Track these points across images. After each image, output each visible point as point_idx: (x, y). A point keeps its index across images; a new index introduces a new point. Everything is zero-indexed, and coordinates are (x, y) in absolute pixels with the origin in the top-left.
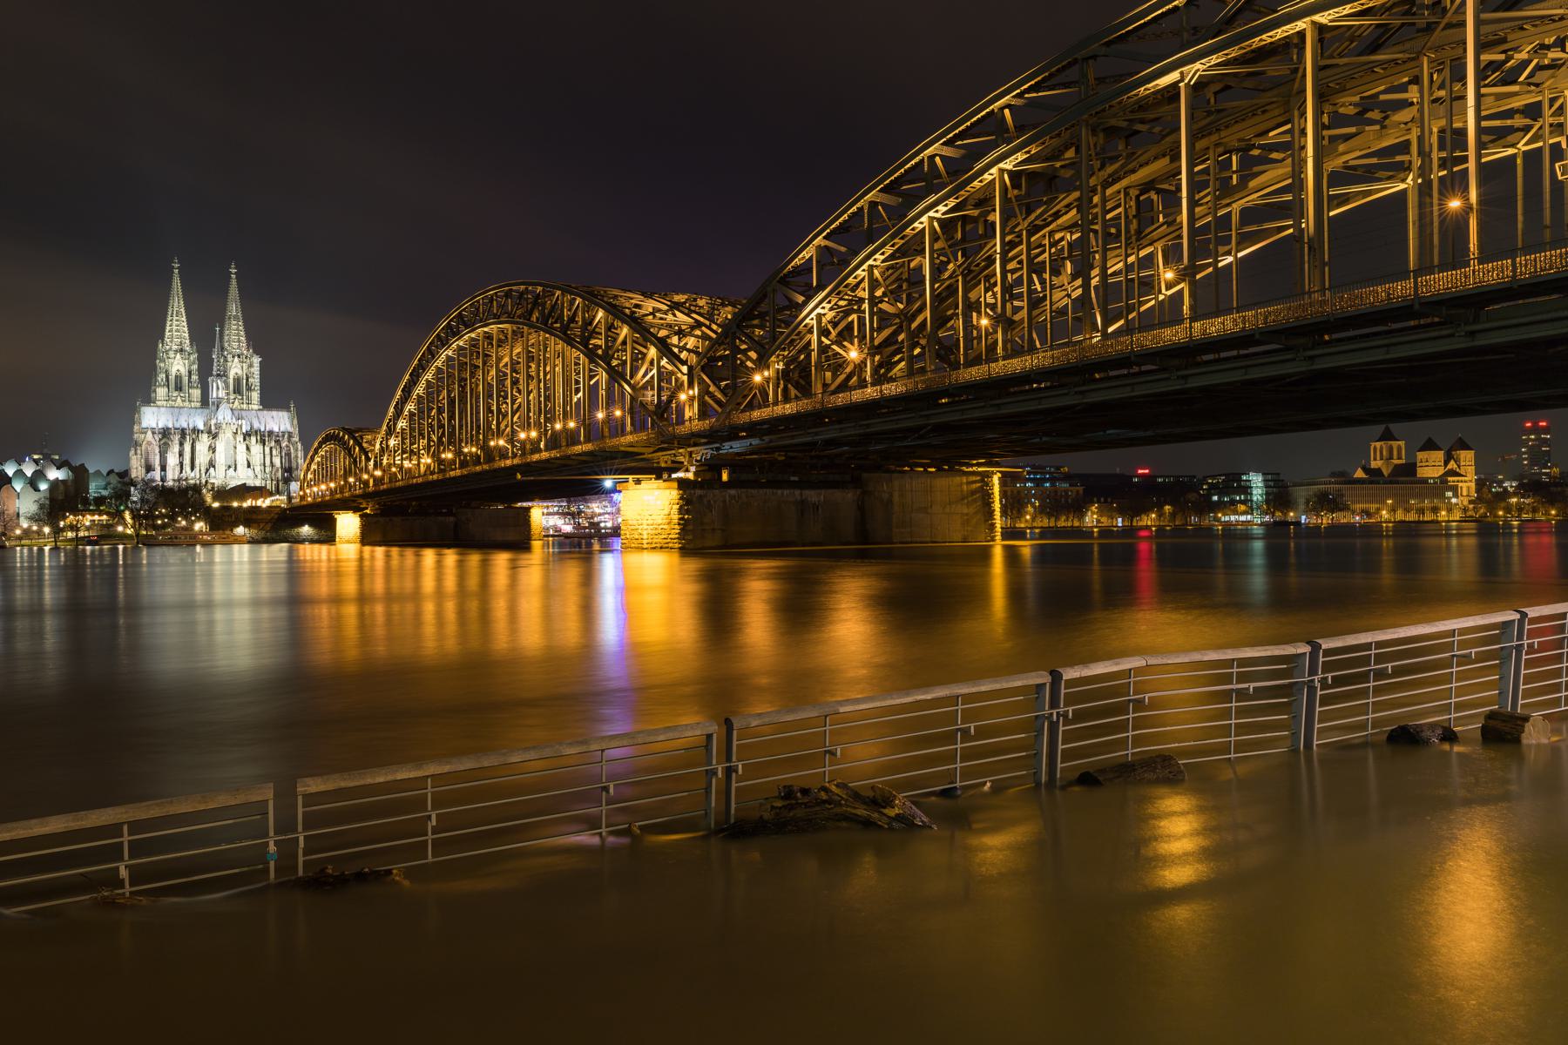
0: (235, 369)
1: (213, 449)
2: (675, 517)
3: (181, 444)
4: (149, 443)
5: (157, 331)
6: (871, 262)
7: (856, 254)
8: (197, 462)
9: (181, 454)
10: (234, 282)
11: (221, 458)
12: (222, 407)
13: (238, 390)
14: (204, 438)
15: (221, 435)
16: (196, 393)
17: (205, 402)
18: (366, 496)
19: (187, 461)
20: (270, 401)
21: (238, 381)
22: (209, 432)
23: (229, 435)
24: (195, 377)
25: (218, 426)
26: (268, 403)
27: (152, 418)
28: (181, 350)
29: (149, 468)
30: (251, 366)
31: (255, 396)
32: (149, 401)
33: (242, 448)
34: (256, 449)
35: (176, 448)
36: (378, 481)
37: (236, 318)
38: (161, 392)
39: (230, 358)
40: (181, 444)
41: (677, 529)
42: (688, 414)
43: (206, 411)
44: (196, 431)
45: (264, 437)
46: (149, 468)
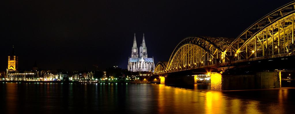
1: (140, 65)
2: (221, 80)
3: (135, 64)
5: (132, 46)
7: (254, 33)
11: (141, 67)
12: (142, 58)
16: (138, 55)
17: (139, 57)
18: (166, 74)
19: (136, 67)
21: (144, 53)
22: (140, 62)
23: (143, 62)
26: (148, 57)
27: (131, 60)
29: (131, 68)
31: (147, 55)
32: (130, 57)
33: (145, 65)
34: (147, 65)
35: (135, 65)
36: (168, 71)
38: (132, 55)
40: (135, 64)
41: (221, 82)
42: (223, 61)
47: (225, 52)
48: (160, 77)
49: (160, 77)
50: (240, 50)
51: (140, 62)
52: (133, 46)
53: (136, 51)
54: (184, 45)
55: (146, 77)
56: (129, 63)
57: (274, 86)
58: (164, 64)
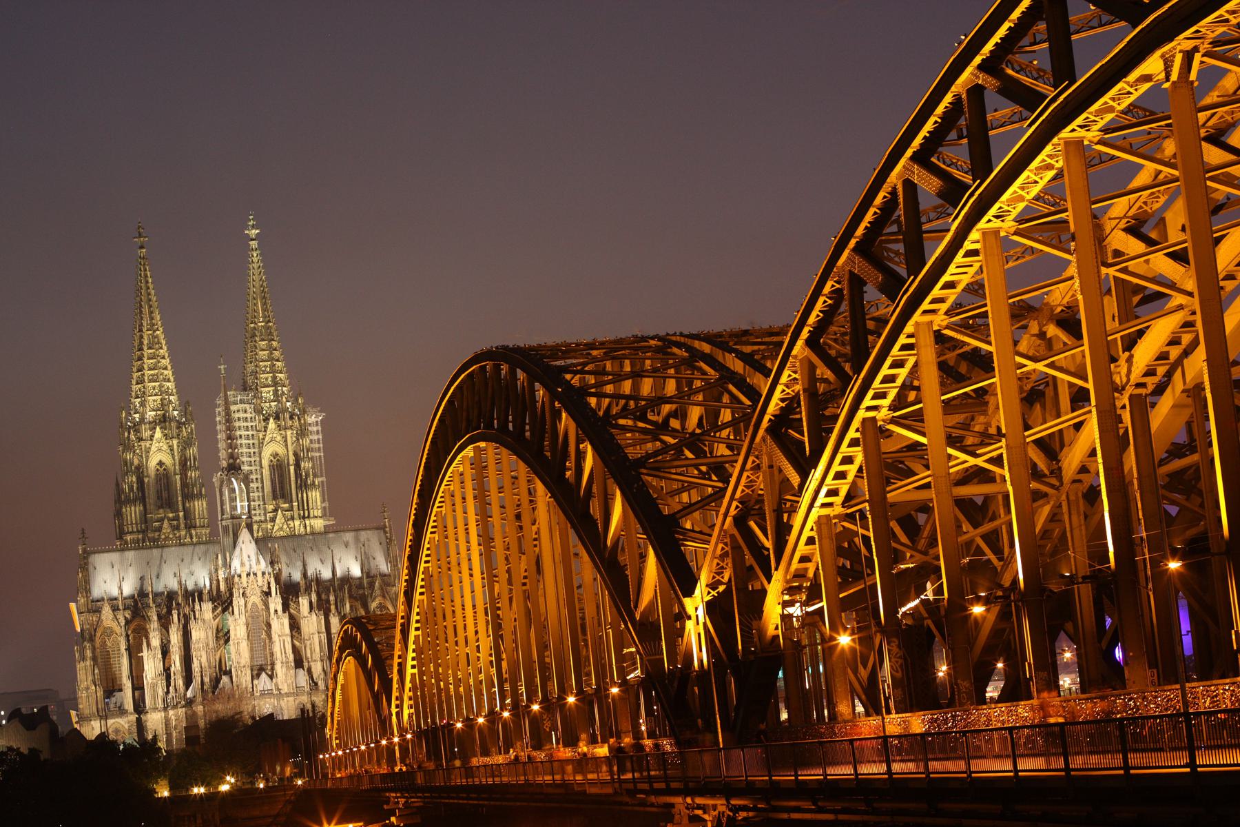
1: (223, 636)
4: (109, 632)
6: (861, 414)
9: (165, 652)
11: (240, 653)
12: (244, 535)
14: (207, 607)
15: (238, 602)
21: (278, 467)
23: (255, 599)
28: (163, 420)
29: (111, 688)
30: (302, 433)
31: (315, 496)
33: (280, 625)
34: (311, 624)
35: (156, 642)
43: (213, 549)
44: (195, 596)
45: (328, 593)
50: (790, 590)
51: (223, 601)
52: (135, 388)
53: (167, 460)
54: (469, 451)
58: (372, 647)
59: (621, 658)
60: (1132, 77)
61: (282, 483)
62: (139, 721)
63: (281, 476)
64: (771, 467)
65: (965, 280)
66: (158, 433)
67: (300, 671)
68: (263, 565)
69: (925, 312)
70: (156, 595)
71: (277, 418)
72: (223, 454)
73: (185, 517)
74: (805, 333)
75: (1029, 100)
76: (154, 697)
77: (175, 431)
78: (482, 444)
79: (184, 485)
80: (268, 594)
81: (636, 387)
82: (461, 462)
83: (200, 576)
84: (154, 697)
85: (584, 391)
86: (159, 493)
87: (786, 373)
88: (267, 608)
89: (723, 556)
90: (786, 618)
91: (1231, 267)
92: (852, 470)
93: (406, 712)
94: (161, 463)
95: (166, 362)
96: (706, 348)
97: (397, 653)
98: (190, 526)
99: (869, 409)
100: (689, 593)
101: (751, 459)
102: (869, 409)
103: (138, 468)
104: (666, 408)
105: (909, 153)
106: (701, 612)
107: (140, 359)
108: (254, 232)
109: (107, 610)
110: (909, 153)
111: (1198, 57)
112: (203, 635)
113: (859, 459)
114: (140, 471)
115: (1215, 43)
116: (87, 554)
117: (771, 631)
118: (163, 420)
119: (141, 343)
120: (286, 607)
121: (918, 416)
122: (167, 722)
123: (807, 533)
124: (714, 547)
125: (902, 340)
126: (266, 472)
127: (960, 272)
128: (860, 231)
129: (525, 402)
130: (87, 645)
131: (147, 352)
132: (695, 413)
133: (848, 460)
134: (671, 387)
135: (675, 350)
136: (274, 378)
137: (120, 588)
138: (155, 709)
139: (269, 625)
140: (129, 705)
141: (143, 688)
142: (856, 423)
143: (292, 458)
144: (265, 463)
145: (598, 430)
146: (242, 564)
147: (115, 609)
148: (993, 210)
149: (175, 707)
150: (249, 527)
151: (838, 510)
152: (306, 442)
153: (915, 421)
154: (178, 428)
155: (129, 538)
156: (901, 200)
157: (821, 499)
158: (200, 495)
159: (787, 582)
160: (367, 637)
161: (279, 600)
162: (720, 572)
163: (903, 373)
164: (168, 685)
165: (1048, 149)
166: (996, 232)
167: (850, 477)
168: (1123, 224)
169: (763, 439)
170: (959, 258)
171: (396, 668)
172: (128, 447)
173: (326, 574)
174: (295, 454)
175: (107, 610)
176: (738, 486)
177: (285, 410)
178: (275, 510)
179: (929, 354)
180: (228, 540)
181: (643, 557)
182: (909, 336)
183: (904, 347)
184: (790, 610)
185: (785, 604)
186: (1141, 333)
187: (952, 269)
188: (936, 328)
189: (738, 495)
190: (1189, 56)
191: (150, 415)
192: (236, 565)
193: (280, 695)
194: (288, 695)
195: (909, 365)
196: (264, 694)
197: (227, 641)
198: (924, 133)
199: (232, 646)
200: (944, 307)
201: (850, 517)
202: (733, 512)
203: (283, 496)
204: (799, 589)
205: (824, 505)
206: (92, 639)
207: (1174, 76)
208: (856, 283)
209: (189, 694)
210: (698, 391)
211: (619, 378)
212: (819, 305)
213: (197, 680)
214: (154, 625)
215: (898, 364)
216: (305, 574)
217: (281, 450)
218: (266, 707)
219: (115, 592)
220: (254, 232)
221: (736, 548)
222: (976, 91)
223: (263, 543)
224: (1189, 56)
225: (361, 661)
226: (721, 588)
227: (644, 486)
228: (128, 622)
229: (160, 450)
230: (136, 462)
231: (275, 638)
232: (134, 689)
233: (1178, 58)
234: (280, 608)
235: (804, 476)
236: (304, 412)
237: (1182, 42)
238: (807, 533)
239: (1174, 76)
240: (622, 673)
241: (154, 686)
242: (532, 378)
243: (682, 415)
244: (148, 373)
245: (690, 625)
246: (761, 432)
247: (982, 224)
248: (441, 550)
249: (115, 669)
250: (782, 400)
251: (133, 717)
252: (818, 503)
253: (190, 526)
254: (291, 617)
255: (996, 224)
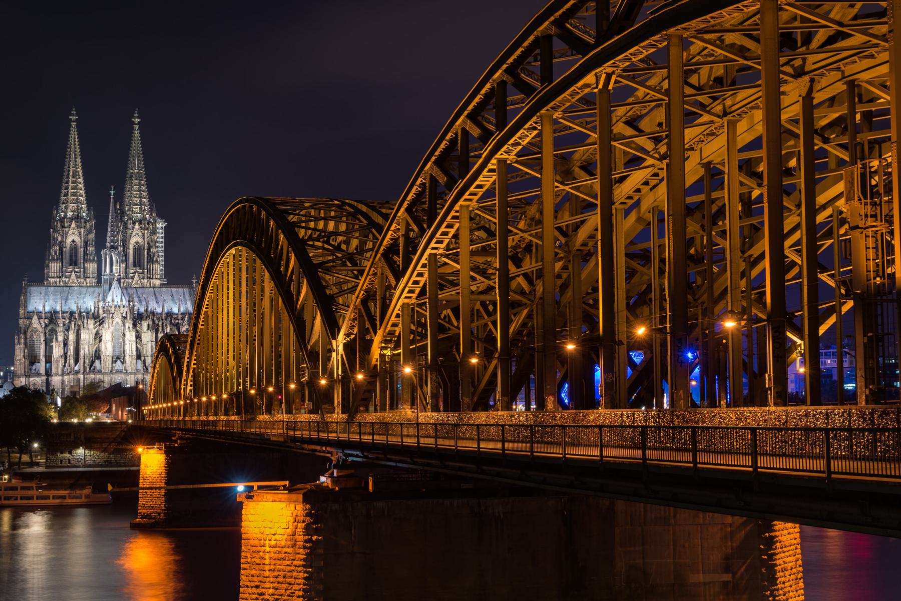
0: (136, 238)
1: (98, 337)
2: (300, 538)
6: (429, 251)
8: (82, 353)
9: (65, 344)
10: (137, 134)
11: (107, 349)
12: (115, 284)
13: (138, 263)
16: (92, 267)
20: (175, 276)
21: (138, 250)
23: (118, 320)
24: (91, 249)
25: (107, 310)
27: (40, 301)
28: (77, 218)
29: (33, 360)
30: (154, 232)
31: (158, 269)
32: (40, 278)
33: (131, 336)
35: (61, 338)
37: (139, 177)
38: (54, 267)
39: (129, 226)
43: (98, 290)
45: (156, 321)
46: (33, 360)
47: (341, 337)
48: (140, 450)
49: (140, 450)
51: (99, 320)
53: (77, 240)
54: (233, 251)
55: (91, 436)
56: (21, 321)
57: (727, 577)
58: (175, 352)
59: (299, 369)
60: (579, 84)
61: (139, 259)
62: (47, 380)
63: (139, 255)
64: (382, 274)
65: (488, 184)
66: (73, 225)
67: (139, 361)
68: (124, 302)
69: (466, 200)
70: (64, 312)
71: (140, 223)
72: (108, 239)
73: (84, 272)
74: (405, 205)
75: (528, 90)
76: (57, 368)
77: (83, 224)
78: (240, 248)
79: (85, 254)
80: (125, 318)
81: (326, 225)
82: (229, 256)
83: (89, 303)
84: (57, 368)
85: (296, 225)
86: (71, 256)
87: (394, 225)
88: (124, 326)
89: (354, 320)
90: (382, 356)
91: (631, 193)
92: (422, 280)
93: (189, 388)
94: (73, 241)
95: (81, 186)
96: (364, 208)
97: (187, 356)
98: (85, 277)
99: (433, 248)
100: (334, 338)
101: (373, 269)
102: (433, 248)
103: (60, 242)
104: (340, 238)
105: (466, 113)
106: (341, 348)
107: (67, 182)
108: (137, 120)
109: (35, 317)
110: (466, 113)
111: (614, 78)
112: (87, 337)
113: (426, 275)
114: (61, 245)
115: (624, 70)
116: (27, 286)
117: (374, 360)
118: (77, 218)
119: (68, 174)
120: (135, 325)
121: (457, 254)
122: (63, 382)
123: (396, 312)
124: (349, 314)
125: (453, 213)
126: (131, 252)
127: (486, 180)
128: (437, 153)
129: (264, 229)
130: (22, 336)
131: (71, 179)
132: (355, 243)
133: (420, 275)
134: (343, 227)
135: (347, 208)
136: (141, 201)
137: (44, 307)
138: (57, 374)
139: (124, 335)
140: (43, 371)
141: (51, 362)
142: (426, 255)
143: (146, 245)
144: (131, 247)
145: (299, 246)
146: (113, 301)
147: (40, 318)
148: (504, 149)
149: (68, 374)
150: (119, 280)
151: (414, 301)
152: (155, 238)
153: (455, 257)
154: (85, 222)
155: (51, 280)
156: (459, 138)
157: (405, 294)
158: (93, 261)
159: (384, 337)
160: (173, 345)
161: (131, 322)
162: (352, 327)
163: (452, 231)
164: (65, 362)
165: (535, 118)
166: (505, 160)
167: (421, 284)
168: (578, 164)
169: (380, 259)
170: (485, 172)
171: (185, 364)
172: (55, 231)
173: (159, 310)
174: (148, 243)
175: (35, 317)
176: (363, 283)
177: (145, 219)
178: (134, 273)
179: (466, 222)
180: (106, 286)
181: (314, 318)
182: (457, 212)
183: (454, 218)
184: (385, 352)
185: (382, 348)
186: (583, 222)
187: (481, 178)
188: (471, 209)
189: (364, 288)
190: (609, 76)
191: (70, 214)
192: (109, 299)
193: (126, 373)
194: (131, 373)
195: (456, 227)
196: (118, 372)
197: (100, 341)
198: (474, 103)
199: (103, 345)
200: (476, 198)
201: (420, 305)
202: (361, 296)
203: (139, 266)
204: (390, 341)
205: (406, 298)
206: (25, 333)
207: (600, 86)
208: (433, 179)
209: (77, 368)
210: (356, 230)
211: (316, 219)
212: (414, 190)
213: (81, 361)
214: (60, 329)
215: (450, 226)
216: (146, 310)
217: (140, 240)
218: (118, 379)
219: (41, 309)
220: (137, 120)
221: (361, 316)
222: (502, 83)
223: (126, 289)
224: (609, 76)
225: (169, 359)
226: (352, 337)
227: (319, 279)
228: (46, 326)
229: (73, 233)
230: (60, 239)
231: (127, 341)
232: (46, 362)
233: (604, 76)
234: (131, 326)
235: (398, 280)
236: (155, 221)
237: (607, 68)
238: (396, 312)
239: (600, 86)
240: (299, 377)
241: (58, 362)
242: (269, 214)
243: (347, 243)
244: (70, 191)
245: (334, 354)
246: (379, 256)
247: (498, 156)
248: (215, 303)
249: (37, 350)
250: (392, 239)
251: (44, 378)
252: (403, 296)
253: (85, 277)
254: (137, 332)
255: (505, 156)
